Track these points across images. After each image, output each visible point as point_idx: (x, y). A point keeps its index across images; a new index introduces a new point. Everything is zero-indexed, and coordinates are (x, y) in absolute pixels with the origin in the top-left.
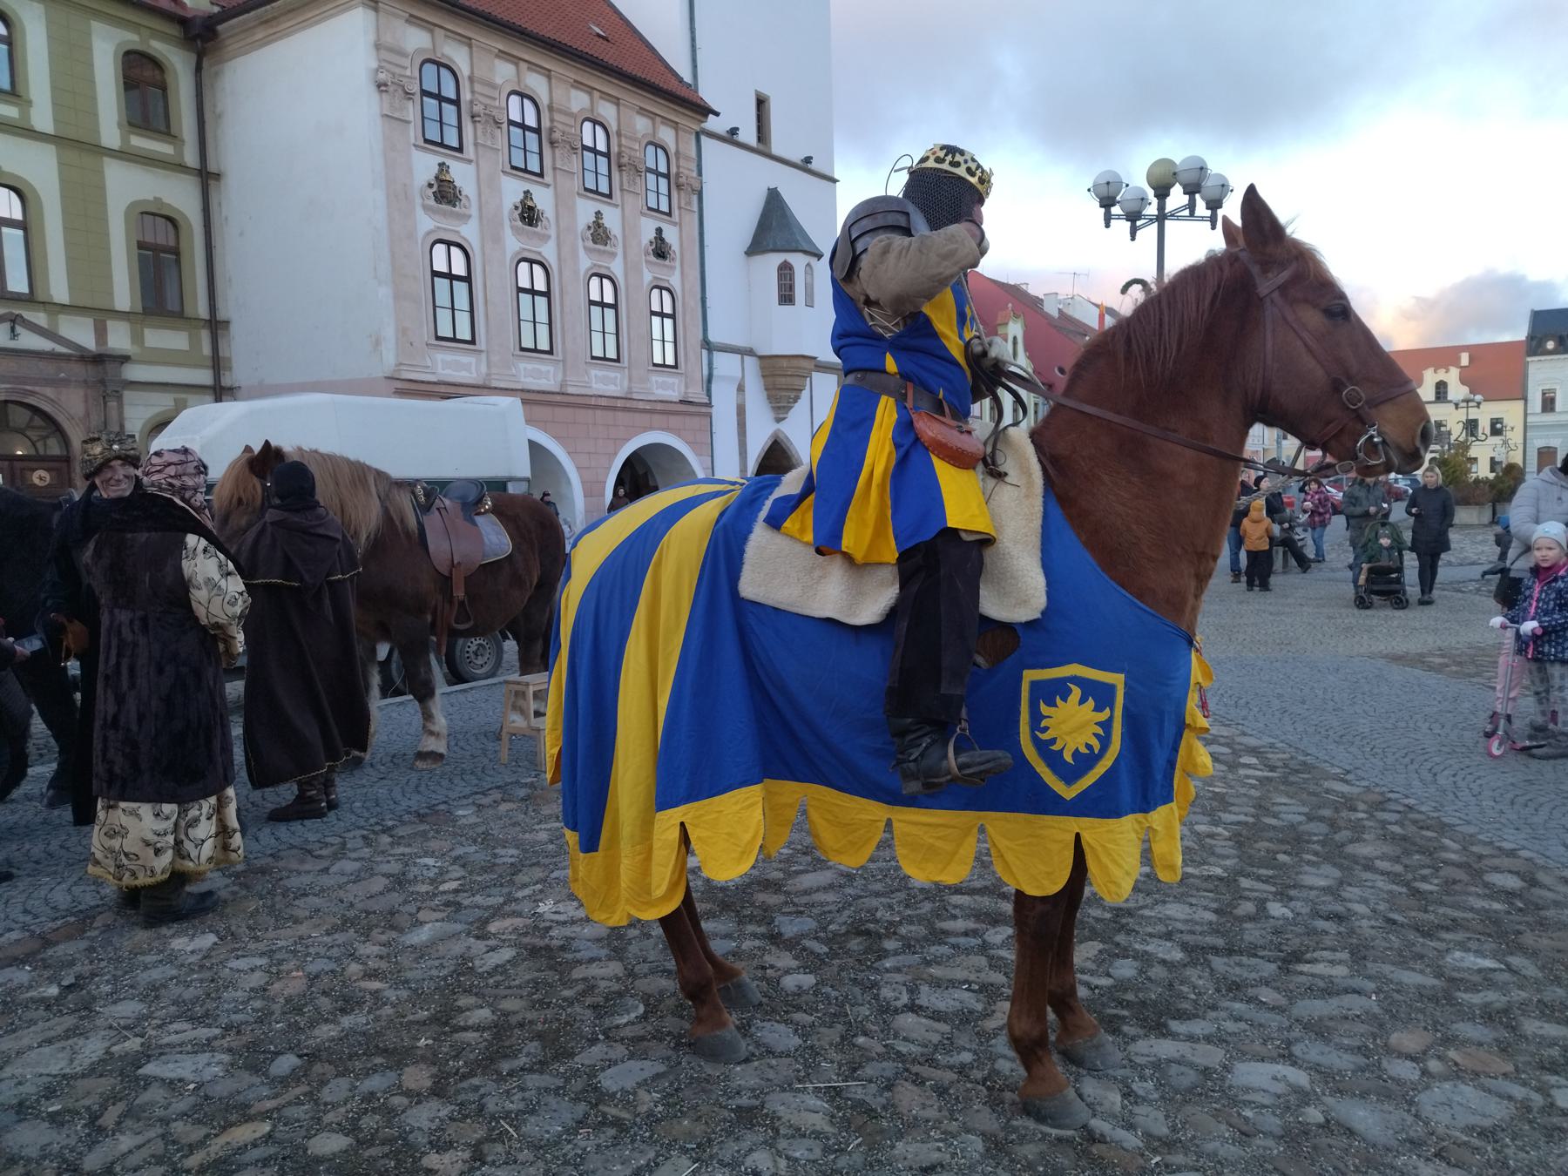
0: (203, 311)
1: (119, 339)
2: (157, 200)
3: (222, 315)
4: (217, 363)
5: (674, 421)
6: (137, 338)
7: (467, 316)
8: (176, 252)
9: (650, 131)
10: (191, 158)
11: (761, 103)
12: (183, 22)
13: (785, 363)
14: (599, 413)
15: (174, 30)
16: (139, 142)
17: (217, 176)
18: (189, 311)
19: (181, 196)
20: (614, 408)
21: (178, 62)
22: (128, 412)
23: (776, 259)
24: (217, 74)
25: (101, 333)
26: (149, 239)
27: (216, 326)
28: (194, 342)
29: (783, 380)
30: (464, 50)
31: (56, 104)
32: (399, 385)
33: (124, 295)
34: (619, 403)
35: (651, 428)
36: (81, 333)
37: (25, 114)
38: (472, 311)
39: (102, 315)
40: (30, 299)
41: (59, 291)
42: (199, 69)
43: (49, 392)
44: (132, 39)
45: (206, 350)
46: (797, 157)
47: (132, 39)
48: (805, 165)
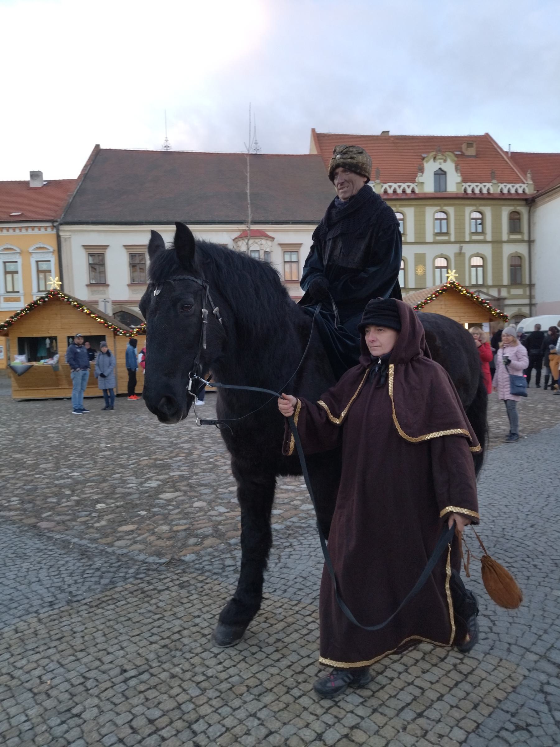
0: (527, 282)
1: (504, 293)
2: (516, 252)
3: (533, 282)
4: (531, 297)
6: (509, 292)
8: (520, 266)
10: (526, 238)
12: (526, 200)
15: (524, 203)
16: (513, 237)
17: (533, 241)
18: (523, 283)
19: (522, 249)
21: (524, 210)
24: (535, 212)
25: (499, 292)
26: (513, 263)
27: (531, 286)
28: (525, 292)
31: (493, 232)
33: (506, 280)
36: (494, 293)
37: (485, 238)
39: (499, 287)
40: (482, 286)
41: (490, 282)
42: (529, 212)
44: (511, 208)
45: (528, 293)
47: (511, 208)
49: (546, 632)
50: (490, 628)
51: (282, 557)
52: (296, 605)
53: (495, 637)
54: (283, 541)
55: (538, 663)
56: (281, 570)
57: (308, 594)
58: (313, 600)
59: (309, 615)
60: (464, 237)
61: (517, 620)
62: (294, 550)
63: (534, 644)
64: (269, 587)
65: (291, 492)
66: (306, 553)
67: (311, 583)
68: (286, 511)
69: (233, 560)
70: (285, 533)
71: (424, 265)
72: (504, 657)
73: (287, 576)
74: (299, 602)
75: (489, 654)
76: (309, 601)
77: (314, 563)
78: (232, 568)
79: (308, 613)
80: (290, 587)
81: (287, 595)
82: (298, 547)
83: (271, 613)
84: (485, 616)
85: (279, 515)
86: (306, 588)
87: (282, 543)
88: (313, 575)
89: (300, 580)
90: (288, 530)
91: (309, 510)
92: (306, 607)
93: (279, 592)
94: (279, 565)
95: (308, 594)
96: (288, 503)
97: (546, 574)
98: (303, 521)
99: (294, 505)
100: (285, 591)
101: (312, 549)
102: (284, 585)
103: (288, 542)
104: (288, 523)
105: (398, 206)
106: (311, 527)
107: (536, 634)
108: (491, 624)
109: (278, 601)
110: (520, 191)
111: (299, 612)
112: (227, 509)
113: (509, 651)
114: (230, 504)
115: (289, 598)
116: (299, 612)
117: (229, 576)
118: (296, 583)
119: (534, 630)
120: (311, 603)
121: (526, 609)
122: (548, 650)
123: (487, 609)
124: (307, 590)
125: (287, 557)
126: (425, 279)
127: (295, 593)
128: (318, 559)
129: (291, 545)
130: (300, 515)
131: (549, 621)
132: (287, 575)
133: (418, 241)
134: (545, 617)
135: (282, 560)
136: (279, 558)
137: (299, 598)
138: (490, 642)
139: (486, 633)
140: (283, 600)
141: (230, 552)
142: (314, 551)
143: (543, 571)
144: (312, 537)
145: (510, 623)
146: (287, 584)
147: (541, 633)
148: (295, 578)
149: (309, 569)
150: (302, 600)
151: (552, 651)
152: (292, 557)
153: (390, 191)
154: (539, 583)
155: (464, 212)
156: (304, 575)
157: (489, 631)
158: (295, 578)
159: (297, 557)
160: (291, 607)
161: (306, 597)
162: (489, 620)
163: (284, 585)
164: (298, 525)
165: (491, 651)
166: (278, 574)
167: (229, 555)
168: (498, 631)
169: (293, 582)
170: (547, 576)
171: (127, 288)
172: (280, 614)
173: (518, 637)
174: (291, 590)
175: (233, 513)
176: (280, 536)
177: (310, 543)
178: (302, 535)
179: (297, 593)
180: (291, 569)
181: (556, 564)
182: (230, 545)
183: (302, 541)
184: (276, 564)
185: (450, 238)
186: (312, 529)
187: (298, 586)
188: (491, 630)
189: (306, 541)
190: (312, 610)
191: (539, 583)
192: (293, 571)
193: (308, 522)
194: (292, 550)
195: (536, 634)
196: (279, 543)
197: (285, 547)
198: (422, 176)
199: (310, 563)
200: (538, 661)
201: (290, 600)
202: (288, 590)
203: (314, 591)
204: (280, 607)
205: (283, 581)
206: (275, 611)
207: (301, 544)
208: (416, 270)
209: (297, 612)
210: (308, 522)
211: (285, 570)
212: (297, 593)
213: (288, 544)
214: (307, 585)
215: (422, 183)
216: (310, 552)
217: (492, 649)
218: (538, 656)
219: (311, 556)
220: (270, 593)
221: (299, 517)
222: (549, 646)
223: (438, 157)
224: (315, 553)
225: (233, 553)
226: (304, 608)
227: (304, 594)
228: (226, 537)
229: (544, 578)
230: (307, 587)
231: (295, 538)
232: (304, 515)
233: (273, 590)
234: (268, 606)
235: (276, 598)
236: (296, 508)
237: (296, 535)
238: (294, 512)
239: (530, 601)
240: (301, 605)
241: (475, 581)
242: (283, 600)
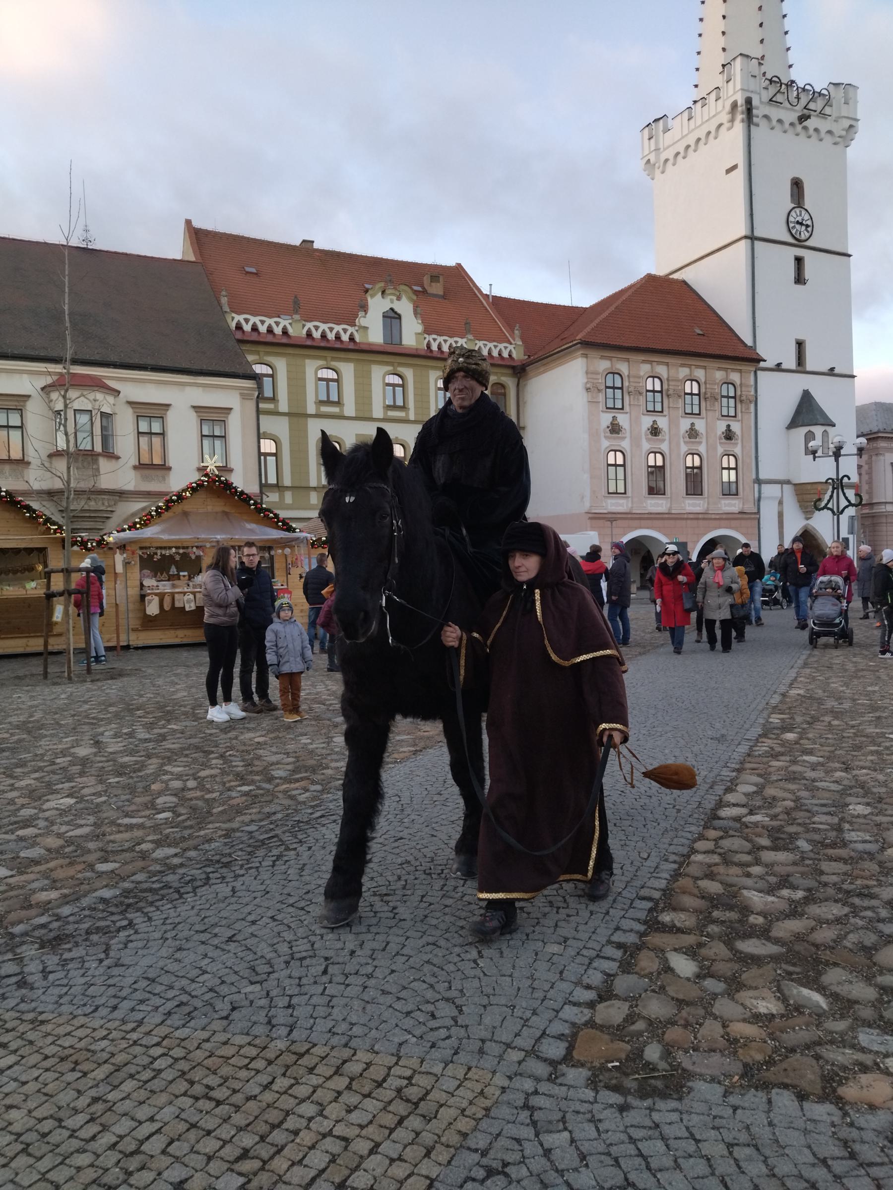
5: (734, 523)
7: (623, 482)
9: (725, 376)
11: (800, 345)
13: (809, 487)
14: (689, 522)
20: (697, 519)
23: (804, 430)
24: (525, 385)
29: (809, 496)
32: (590, 515)
34: (700, 516)
35: (720, 528)
38: (625, 480)
46: (825, 369)
48: (831, 372)
49: (535, 1013)
50: (454, 1019)
51: (113, 947)
52: (134, 1030)
53: (462, 1032)
54: (115, 918)
55: (524, 1063)
56: (109, 971)
57: (157, 1008)
58: (165, 1017)
59: (158, 1044)
61: (494, 1000)
62: (136, 932)
63: (517, 1035)
64: (85, 1005)
65: (138, 829)
66: (157, 935)
67: (164, 988)
68: (126, 863)
69: (18, 964)
70: (122, 903)
72: (474, 1064)
73: (121, 981)
74: (140, 1023)
75: (452, 1062)
76: (158, 1018)
77: (171, 950)
78: (14, 979)
79: (156, 1040)
80: (125, 998)
81: (118, 1014)
82: (143, 927)
83: (85, 1052)
84: (447, 1000)
85: (112, 871)
86: (153, 998)
87: (114, 922)
88: (167, 972)
89: (143, 984)
90: (126, 897)
91: (168, 858)
92: (151, 1031)
93: (103, 1012)
94: (106, 963)
95: (157, 1008)
96: (131, 849)
97: (536, 921)
98: (155, 879)
99: (141, 852)
100: (115, 1008)
101: (169, 927)
102: (115, 996)
103: (126, 919)
104: (127, 885)
105: (329, 359)
106: (170, 887)
107: (521, 1018)
108: (455, 1013)
109: (101, 1027)
110: (505, 354)
111: (139, 1042)
112: (12, 870)
113: (481, 1052)
114: (19, 860)
115: (123, 1020)
116: (139, 1042)
117: (7, 995)
118: (136, 990)
119: (518, 1012)
120: (163, 1022)
121: (508, 979)
122: (538, 1040)
123: (450, 987)
124: (157, 1001)
125: (121, 946)
127: (133, 1010)
128: (178, 942)
129: (131, 924)
130: (150, 868)
131: (539, 994)
132: (120, 978)
134: (534, 988)
135: (112, 954)
136: (106, 951)
137: (140, 1016)
138: (453, 1042)
139: (448, 1029)
140: (110, 1025)
141: (12, 950)
142: (173, 929)
143: (531, 916)
144: (169, 906)
145: (485, 1006)
146: (119, 994)
147: (528, 1014)
148: (135, 982)
149: (161, 964)
150: (145, 1020)
151: (543, 1041)
152: (130, 945)
153: (317, 335)
154: (527, 935)
156: (151, 975)
157: (452, 1023)
158: (135, 982)
159: (140, 944)
160: (123, 1034)
161: (152, 1014)
162: (453, 1006)
163: (115, 996)
164: (145, 886)
165: (455, 1057)
166: (103, 978)
167: (10, 956)
168: (467, 1022)
169: (130, 990)
170: (538, 923)
172: (103, 1050)
173: (495, 1027)
174: (126, 1005)
175: (23, 878)
176: (113, 909)
177: (165, 916)
178: (151, 904)
179: (137, 1008)
180: (129, 966)
181: (550, 902)
182: (12, 936)
183: (150, 915)
184: (101, 961)
185: (407, 414)
186: (172, 890)
187: (138, 995)
188: (456, 1022)
189: (159, 913)
190: (163, 1035)
191: (527, 935)
192: (130, 970)
193: (165, 879)
194: (132, 932)
195: (521, 1018)
196: (108, 923)
197: (118, 930)
198: (365, 317)
199: (164, 952)
200: (524, 1060)
201: (124, 1022)
202: (119, 1006)
203: (168, 1000)
204: (104, 1038)
205: (112, 991)
206: (92, 1047)
207: (150, 919)
209: (135, 1043)
210: (165, 879)
211: (116, 971)
212: (137, 1008)
213: (125, 923)
214: (156, 991)
215: (366, 328)
216: (165, 932)
217: (456, 1053)
218: (523, 1053)
219: (167, 939)
220: (85, 1015)
221: (149, 872)
222: (538, 1034)
223: (387, 292)
224: (174, 933)
225: (18, 951)
226: (148, 1033)
227: (149, 1008)
228: (5, 923)
229: (534, 926)
230: (155, 995)
231: (139, 910)
232: (158, 868)
233: (93, 1008)
234: (81, 1039)
235: (97, 1023)
236: (144, 855)
237: (141, 904)
238: (140, 864)
239: (514, 967)
240: (142, 1029)
241: (434, 944)
242: (110, 1025)
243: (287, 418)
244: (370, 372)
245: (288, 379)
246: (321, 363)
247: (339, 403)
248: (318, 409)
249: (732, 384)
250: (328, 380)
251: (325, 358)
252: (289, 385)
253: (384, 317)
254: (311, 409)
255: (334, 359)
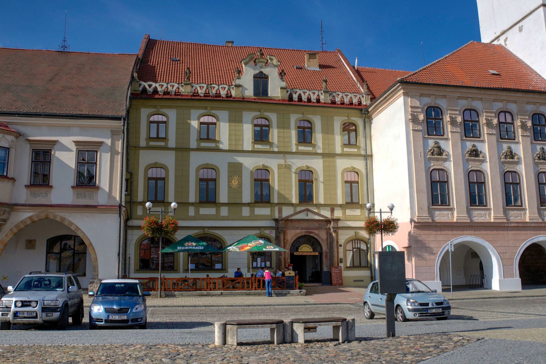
1: (338, 214)
6: (344, 213)
19: (359, 164)
22: (340, 237)
30: (444, 100)
43: (316, 232)
60: (291, 146)
71: (240, 177)
105: (209, 108)
126: (241, 192)
133: (234, 148)
155: (290, 119)
171: (71, 190)
208: (229, 182)
243: (173, 154)
244: (242, 116)
245: (177, 123)
246: (202, 111)
247: (165, 139)
248: (198, 144)
249: (509, 113)
250: (158, 123)
251: (206, 108)
252: (177, 128)
253: (254, 77)
254: (193, 144)
255: (212, 108)
